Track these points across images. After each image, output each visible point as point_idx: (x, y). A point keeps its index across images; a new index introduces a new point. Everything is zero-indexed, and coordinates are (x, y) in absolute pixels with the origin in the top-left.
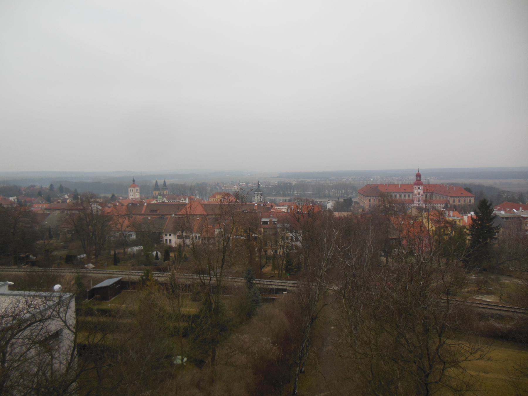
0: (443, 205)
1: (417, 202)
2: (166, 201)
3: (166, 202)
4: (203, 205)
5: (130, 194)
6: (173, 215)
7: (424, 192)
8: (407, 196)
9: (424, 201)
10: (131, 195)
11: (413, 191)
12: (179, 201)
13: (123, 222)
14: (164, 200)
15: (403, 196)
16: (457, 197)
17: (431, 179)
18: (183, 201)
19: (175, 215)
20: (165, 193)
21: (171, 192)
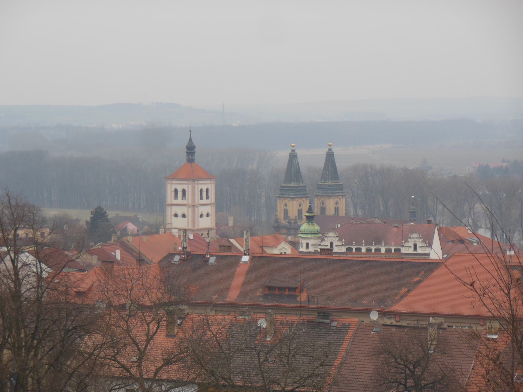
2: (339, 248)
3: (336, 250)
5: (170, 211)
6: (374, 316)
10: (176, 215)
13: (149, 339)
14: (327, 244)
18: (419, 251)
19: (382, 314)
20: (330, 211)
21: (355, 207)
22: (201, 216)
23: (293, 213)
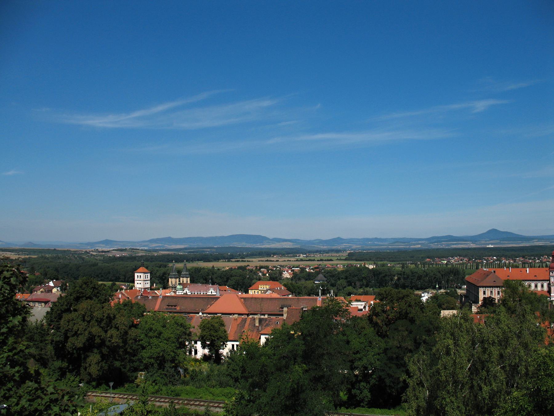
4: (242, 300)
5: (136, 282)
6: (200, 314)
8: (539, 285)
10: (138, 284)
12: (206, 293)
18: (213, 294)
19: (203, 313)
20: (185, 282)
22: (138, 284)
23: (174, 283)
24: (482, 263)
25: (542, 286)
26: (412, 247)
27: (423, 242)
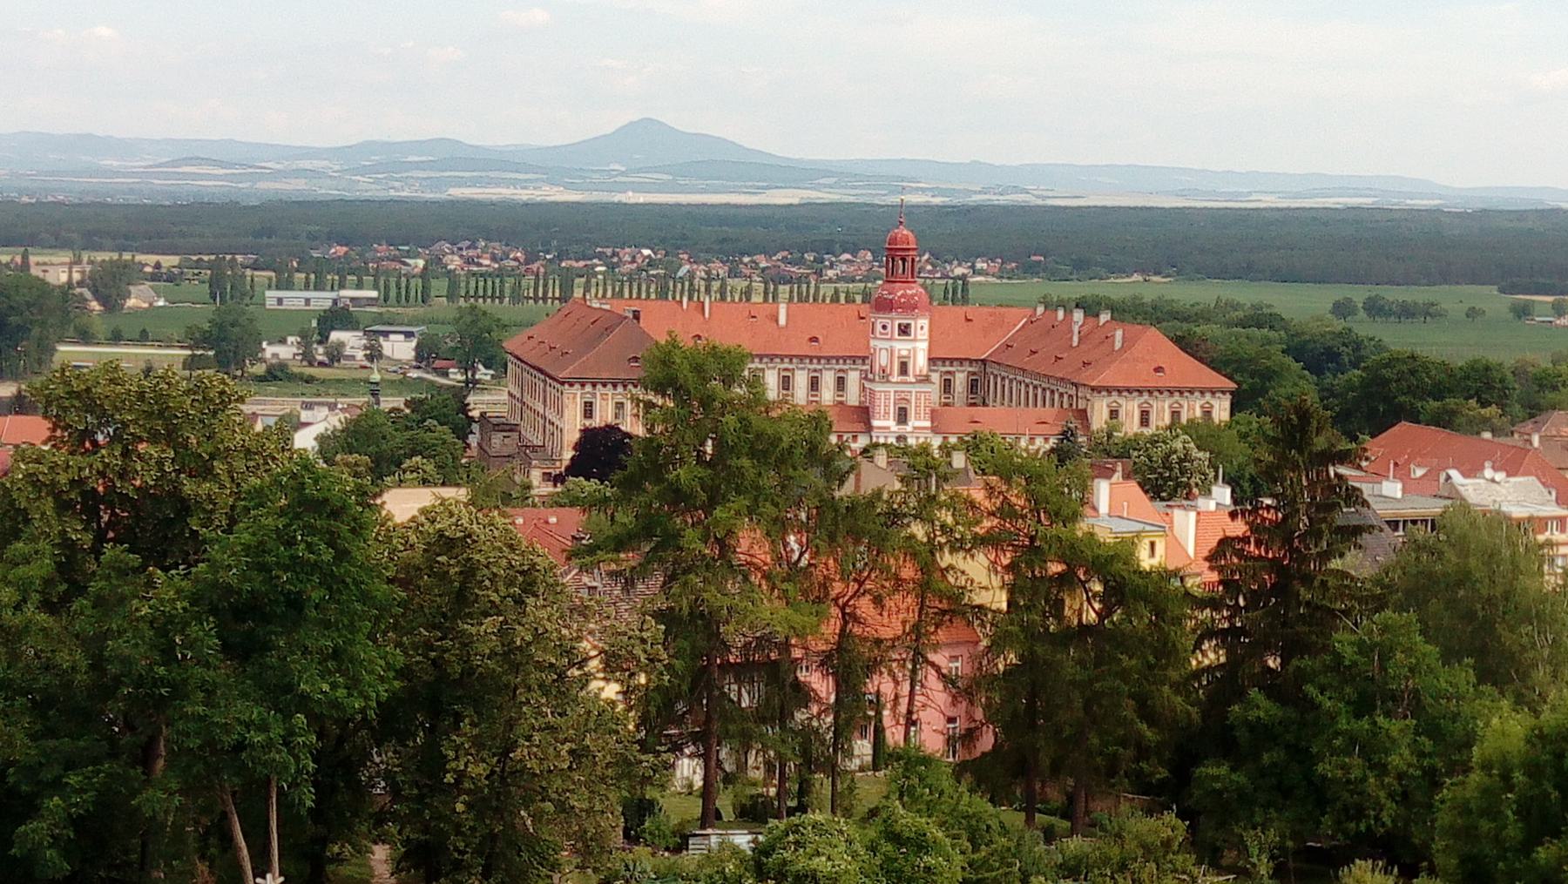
0: (1046, 440)
1: (891, 423)
7: (932, 361)
8: (828, 379)
9: (934, 415)
11: (868, 347)
15: (801, 380)
16: (1129, 391)
17: (976, 272)
24: (589, 273)
25: (841, 383)
26: (262, 185)
27: (317, 164)
